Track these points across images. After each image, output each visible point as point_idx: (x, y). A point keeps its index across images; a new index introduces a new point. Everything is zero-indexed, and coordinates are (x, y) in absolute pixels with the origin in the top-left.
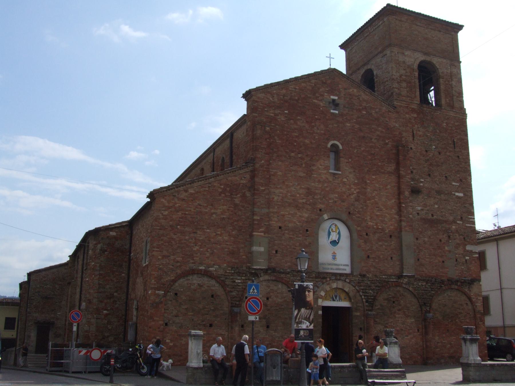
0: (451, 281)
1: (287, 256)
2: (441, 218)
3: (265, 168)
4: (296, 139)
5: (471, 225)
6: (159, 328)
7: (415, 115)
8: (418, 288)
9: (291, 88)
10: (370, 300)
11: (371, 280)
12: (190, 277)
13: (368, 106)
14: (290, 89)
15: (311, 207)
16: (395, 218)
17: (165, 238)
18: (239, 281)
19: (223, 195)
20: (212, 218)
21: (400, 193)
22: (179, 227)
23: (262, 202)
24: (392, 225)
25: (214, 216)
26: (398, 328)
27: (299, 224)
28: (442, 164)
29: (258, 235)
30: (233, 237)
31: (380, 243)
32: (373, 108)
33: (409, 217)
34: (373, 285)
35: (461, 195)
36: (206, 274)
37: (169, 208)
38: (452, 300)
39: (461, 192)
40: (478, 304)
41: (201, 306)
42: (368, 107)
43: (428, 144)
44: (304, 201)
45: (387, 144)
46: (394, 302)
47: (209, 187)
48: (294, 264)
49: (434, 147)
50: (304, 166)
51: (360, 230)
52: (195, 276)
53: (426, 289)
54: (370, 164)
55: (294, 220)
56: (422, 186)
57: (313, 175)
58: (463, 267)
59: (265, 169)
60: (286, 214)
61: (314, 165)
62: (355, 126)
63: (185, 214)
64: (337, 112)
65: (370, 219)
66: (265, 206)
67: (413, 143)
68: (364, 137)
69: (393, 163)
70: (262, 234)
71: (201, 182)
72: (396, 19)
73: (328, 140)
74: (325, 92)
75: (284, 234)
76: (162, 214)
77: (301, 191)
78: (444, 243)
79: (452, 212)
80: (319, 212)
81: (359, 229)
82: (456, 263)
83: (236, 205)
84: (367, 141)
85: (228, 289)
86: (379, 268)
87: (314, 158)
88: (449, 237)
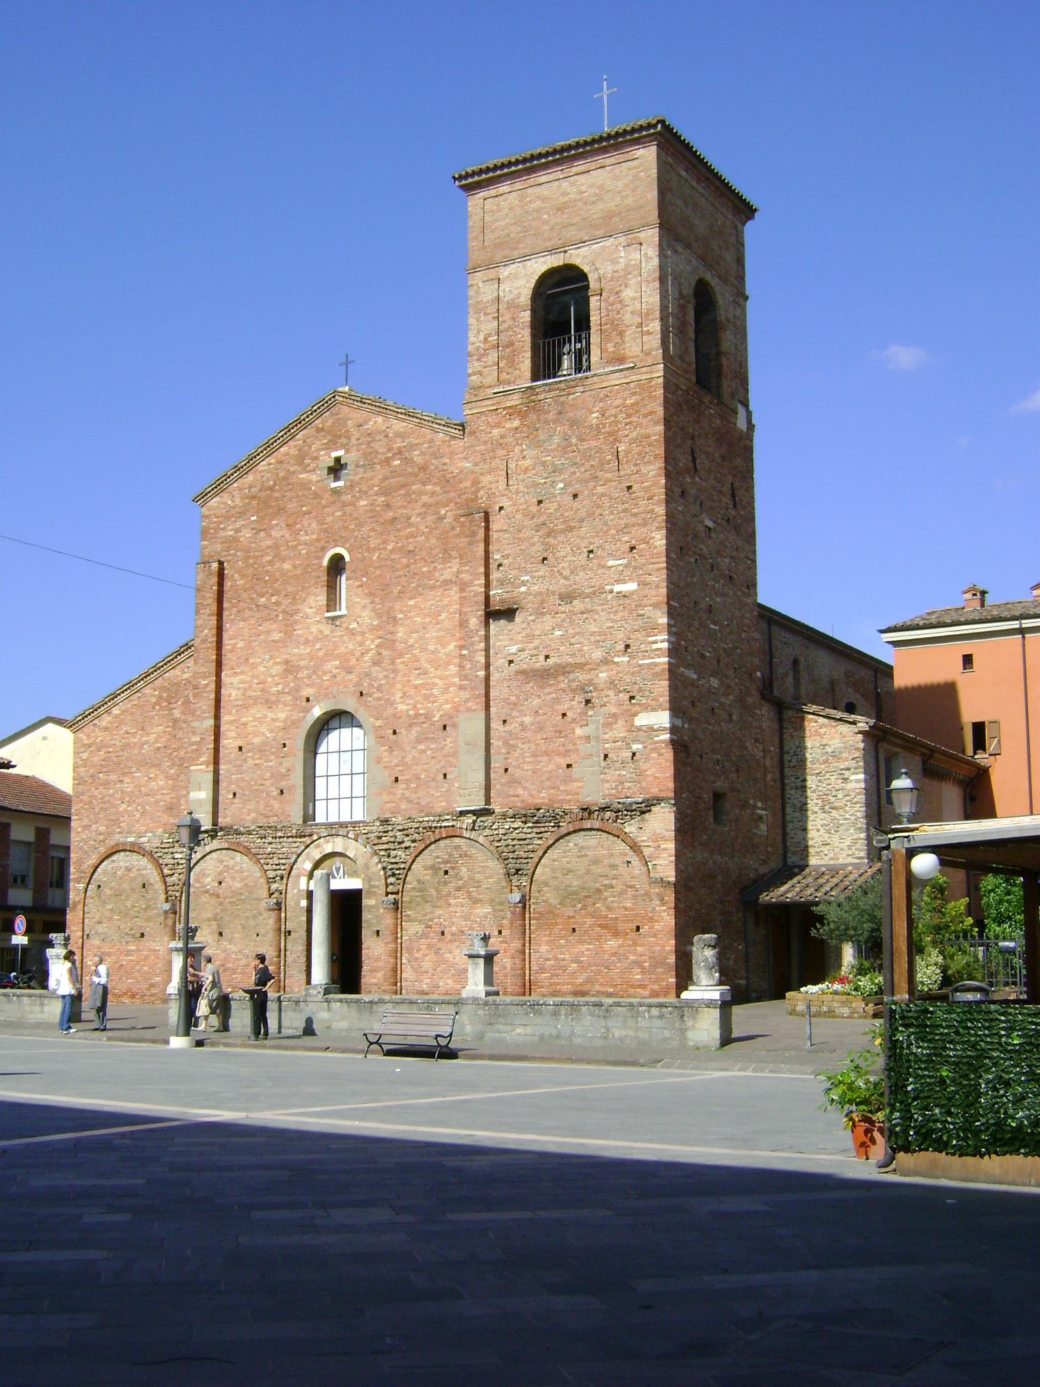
0: (587, 811)
1: (250, 800)
2: (571, 660)
3: (211, 642)
4: (269, 568)
5: (653, 660)
6: (77, 943)
7: (516, 423)
8: (504, 834)
9: (263, 466)
10: (397, 872)
11: (401, 828)
12: (114, 857)
13: (405, 444)
14: (260, 469)
15: (291, 698)
16: (453, 684)
17: (85, 798)
18: (180, 856)
19: (157, 707)
20: (143, 751)
21: (463, 624)
22: (101, 775)
23: (203, 708)
24: (447, 702)
25: (146, 746)
26: (454, 929)
27: (269, 735)
28: (582, 520)
29: (198, 770)
30: (172, 779)
31: (422, 747)
32: (417, 444)
33: (477, 676)
34: (406, 839)
35: (631, 586)
36: (135, 849)
37: (90, 746)
38: (586, 855)
39: (631, 580)
40: (661, 862)
41: (128, 904)
42: (405, 447)
43: (546, 483)
44: (280, 687)
45: (442, 518)
46: (446, 872)
47: (139, 697)
48: (261, 814)
49: (561, 485)
50: (280, 618)
51: (380, 727)
52: (122, 853)
53: (523, 836)
54: (406, 576)
55: (263, 730)
56: (523, 593)
57: (295, 632)
58: (624, 773)
59: (209, 645)
60: (250, 721)
61: (298, 610)
62: (376, 500)
63: (109, 752)
64: (341, 483)
65: (401, 698)
66: (207, 715)
67: (503, 495)
68: (394, 519)
69: (455, 558)
70: (204, 767)
71: (126, 693)
72: (485, 199)
73: (324, 550)
74: (322, 450)
75: (245, 760)
76: (80, 758)
77: (274, 672)
78: (574, 720)
79: (603, 637)
80: (304, 703)
81: (378, 723)
82: (603, 764)
83: (175, 721)
84: (398, 527)
85: (166, 871)
86: (418, 801)
87: (297, 597)
88: (588, 702)
